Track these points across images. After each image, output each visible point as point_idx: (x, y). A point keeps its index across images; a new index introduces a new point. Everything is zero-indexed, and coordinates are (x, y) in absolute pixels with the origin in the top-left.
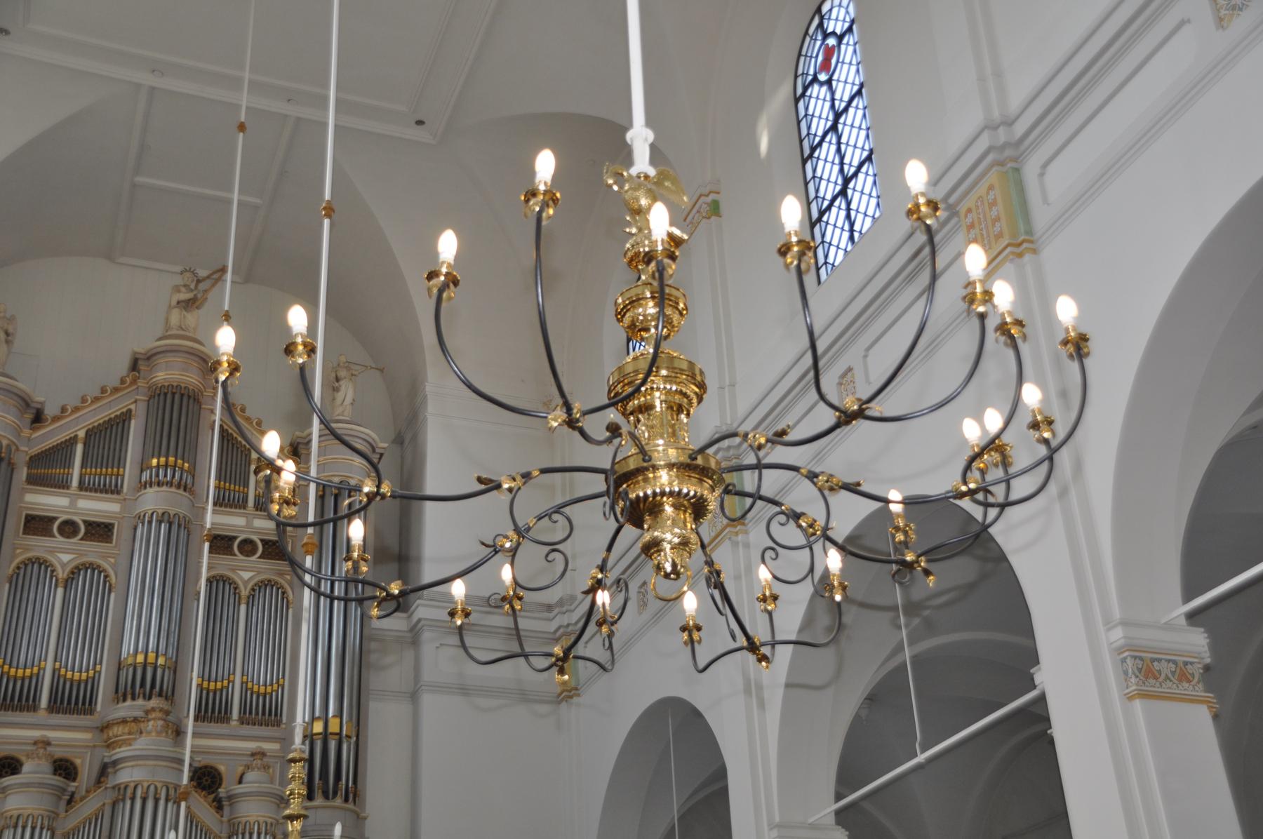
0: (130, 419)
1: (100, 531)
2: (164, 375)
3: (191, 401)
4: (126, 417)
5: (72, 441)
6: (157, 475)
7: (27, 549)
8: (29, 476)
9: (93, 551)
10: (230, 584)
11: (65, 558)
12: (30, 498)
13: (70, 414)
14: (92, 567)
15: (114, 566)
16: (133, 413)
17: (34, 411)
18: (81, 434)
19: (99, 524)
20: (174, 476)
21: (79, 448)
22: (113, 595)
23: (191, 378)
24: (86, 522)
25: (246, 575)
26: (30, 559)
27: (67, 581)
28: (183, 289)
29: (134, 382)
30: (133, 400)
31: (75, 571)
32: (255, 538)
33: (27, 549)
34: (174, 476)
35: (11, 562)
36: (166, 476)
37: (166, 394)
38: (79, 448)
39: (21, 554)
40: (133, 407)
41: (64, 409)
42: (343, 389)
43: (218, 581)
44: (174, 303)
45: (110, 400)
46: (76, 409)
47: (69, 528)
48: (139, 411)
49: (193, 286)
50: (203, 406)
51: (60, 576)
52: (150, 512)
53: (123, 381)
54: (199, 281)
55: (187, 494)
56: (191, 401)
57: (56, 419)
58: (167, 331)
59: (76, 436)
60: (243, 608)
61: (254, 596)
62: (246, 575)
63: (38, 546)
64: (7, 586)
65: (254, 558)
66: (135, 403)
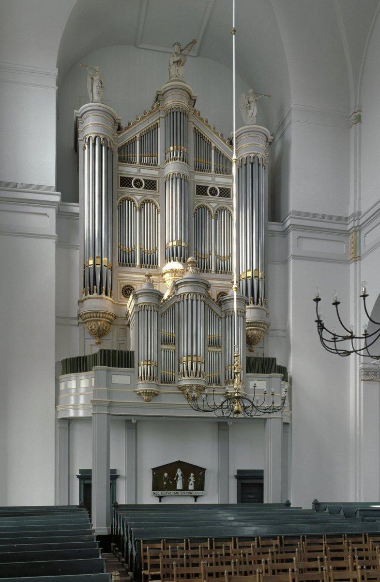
0: (157, 128)
1: (151, 185)
2: (170, 102)
3: (185, 116)
4: (155, 127)
5: (134, 141)
6: (173, 155)
7: (122, 194)
8: (119, 158)
9: (149, 195)
10: (207, 209)
11: (139, 197)
12: (120, 168)
13: (131, 127)
14: (149, 201)
15: (158, 201)
16: (159, 124)
17: (117, 125)
18: (138, 136)
19: (150, 181)
20: (180, 156)
21: (138, 142)
22: (159, 215)
23: (185, 103)
24: (146, 181)
25: (214, 205)
26: (124, 198)
27: (140, 208)
28: (175, 55)
29: (158, 106)
30: (158, 118)
31: (143, 204)
32: (216, 187)
33: (122, 194)
34: (180, 156)
35: (118, 199)
36: (177, 155)
37: (173, 113)
38: (138, 142)
39: (121, 196)
40: (158, 121)
41: (129, 124)
42: (252, 107)
43: (201, 208)
44: (171, 62)
45: (148, 118)
46: (135, 123)
47: (138, 184)
48: (161, 123)
49: (179, 53)
50: (189, 120)
51: (137, 206)
52: (172, 174)
53: (153, 108)
54: (181, 51)
55: (186, 164)
56: (185, 116)
57: (127, 128)
58: (170, 79)
59: (136, 137)
60: (213, 220)
61: (217, 215)
62: (214, 205)
63: (128, 192)
64: (117, 210)
65: (216, 197)
66: (159, 118)
